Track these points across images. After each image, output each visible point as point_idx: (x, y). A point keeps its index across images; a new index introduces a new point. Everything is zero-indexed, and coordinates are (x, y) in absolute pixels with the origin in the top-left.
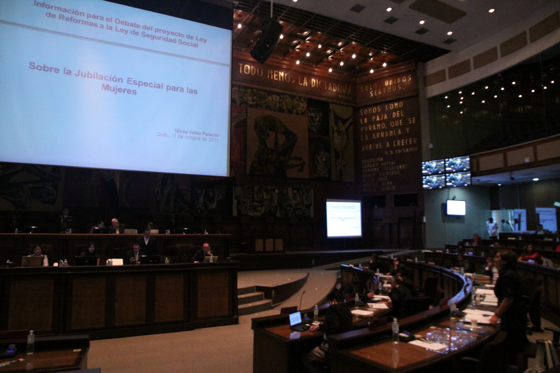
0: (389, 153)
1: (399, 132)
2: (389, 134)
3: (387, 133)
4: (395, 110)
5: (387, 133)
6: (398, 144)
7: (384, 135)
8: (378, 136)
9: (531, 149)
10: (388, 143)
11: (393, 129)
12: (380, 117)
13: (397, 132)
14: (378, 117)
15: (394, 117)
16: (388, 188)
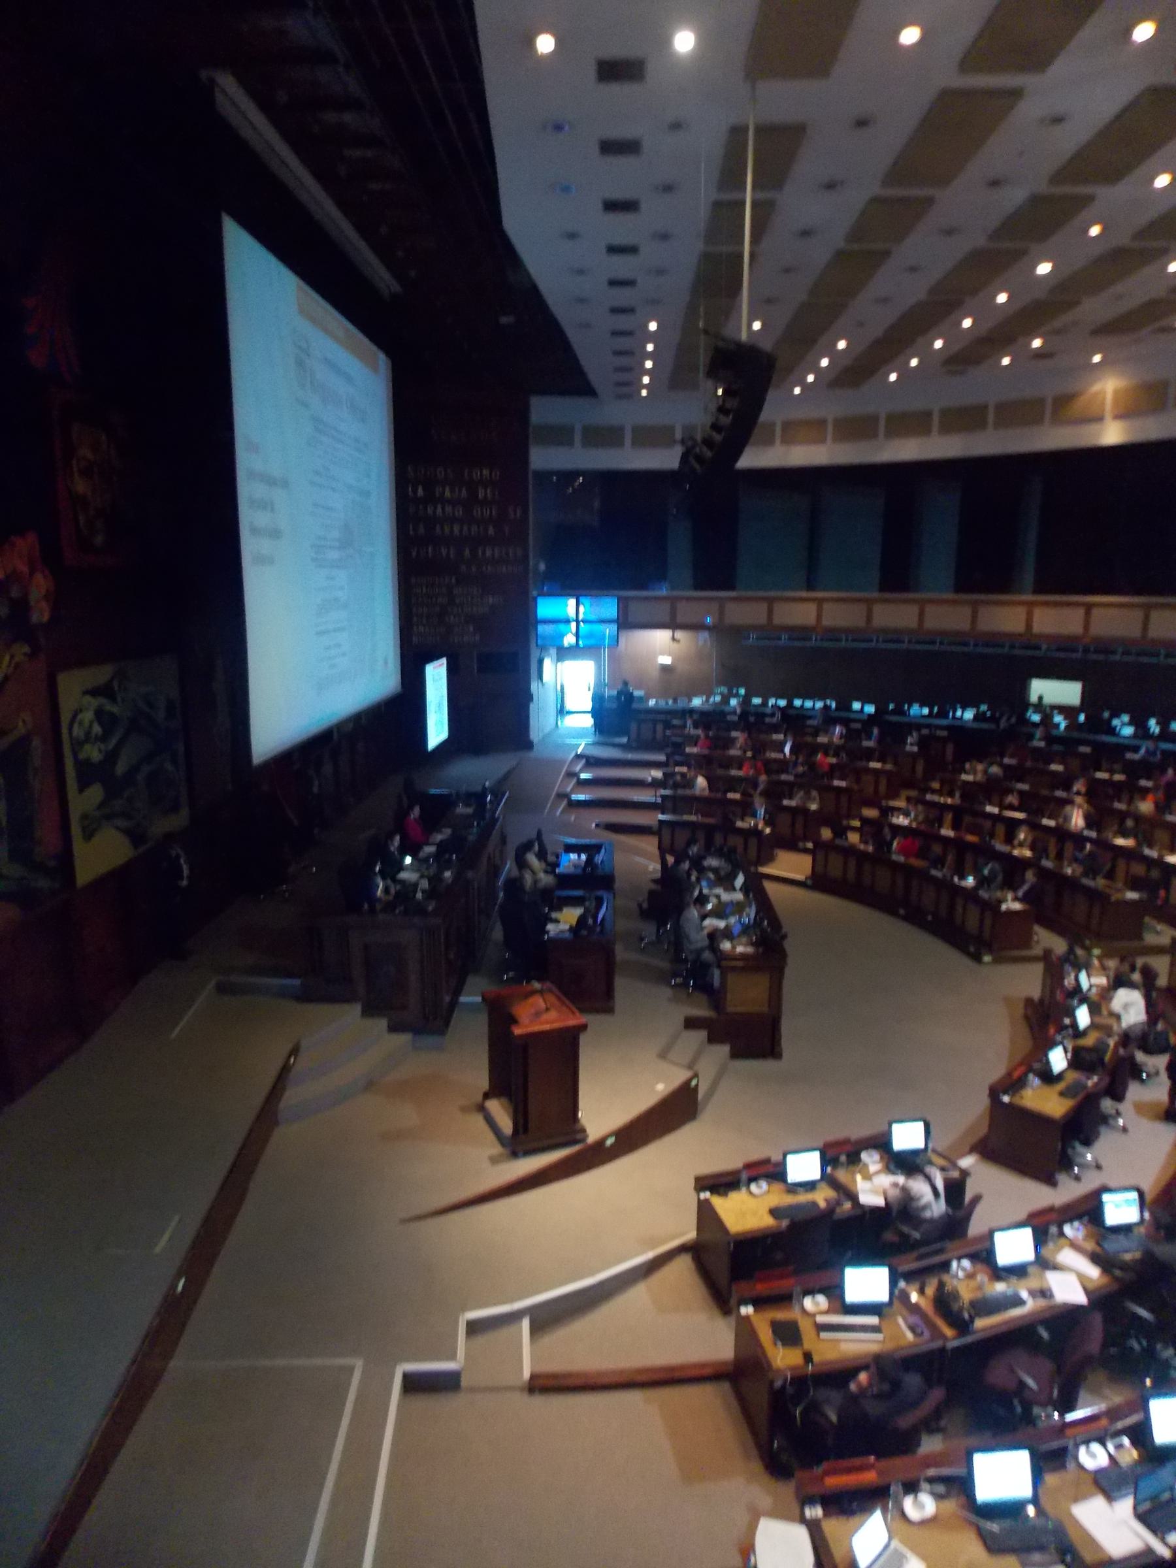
1: (491, 531)
3: (465, 528)
5: (465, 528)
7: (461, 531)
8: (447, 530)
9: (715, 606)
12: (452, 491)
14: (447, 489)
16: (466, 639)
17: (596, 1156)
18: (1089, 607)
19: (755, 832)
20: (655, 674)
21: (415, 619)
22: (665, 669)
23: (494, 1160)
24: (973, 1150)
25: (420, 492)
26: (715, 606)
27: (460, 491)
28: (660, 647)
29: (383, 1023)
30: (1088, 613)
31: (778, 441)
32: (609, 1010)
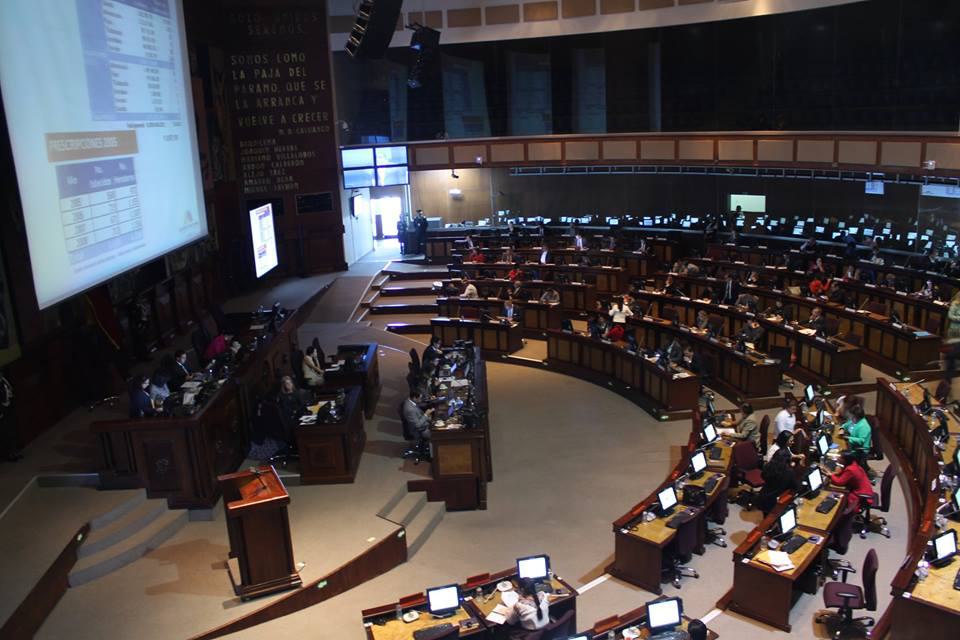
0: (286, 132)
1: (301, 101)
2: (284, 101)
3: (280, 100)
4: (294, 65)
5: (280, 100)
6: (300, 119)
7: (277, 103)
9: (483, 148)
10: (283, 117)
11: (291, 94)
12: (268, 72)
13: (297, 100)
14: (264, 71)
15: (291, 75)
16: (287, 187)
17: (312, 596)
18: (756, 138)
19: (506, 327)
20: (448, 202)
21: (245, 175)
22: (457, 199)
23: (227, 605)
24: (607, 571)
25: (242, 76)
26: (483, 148)
27: (274, 72)
28: (450, 184)
29: (163, 502)
30: (755, 144)
31: (522, 19)
32: (351, 481)
